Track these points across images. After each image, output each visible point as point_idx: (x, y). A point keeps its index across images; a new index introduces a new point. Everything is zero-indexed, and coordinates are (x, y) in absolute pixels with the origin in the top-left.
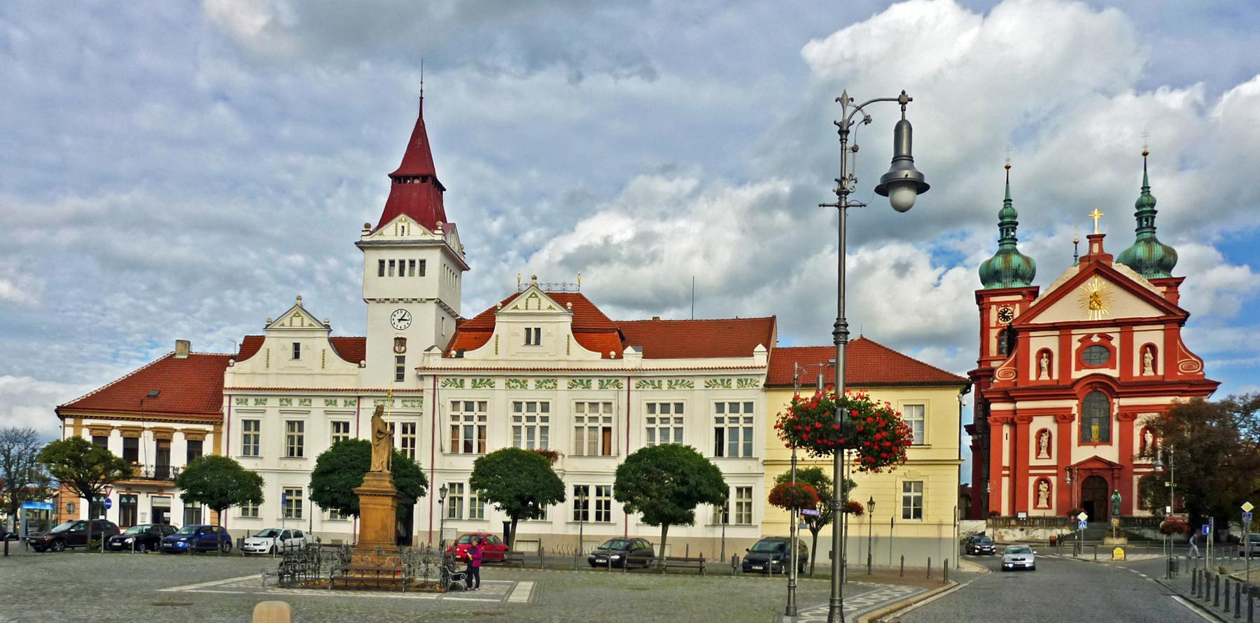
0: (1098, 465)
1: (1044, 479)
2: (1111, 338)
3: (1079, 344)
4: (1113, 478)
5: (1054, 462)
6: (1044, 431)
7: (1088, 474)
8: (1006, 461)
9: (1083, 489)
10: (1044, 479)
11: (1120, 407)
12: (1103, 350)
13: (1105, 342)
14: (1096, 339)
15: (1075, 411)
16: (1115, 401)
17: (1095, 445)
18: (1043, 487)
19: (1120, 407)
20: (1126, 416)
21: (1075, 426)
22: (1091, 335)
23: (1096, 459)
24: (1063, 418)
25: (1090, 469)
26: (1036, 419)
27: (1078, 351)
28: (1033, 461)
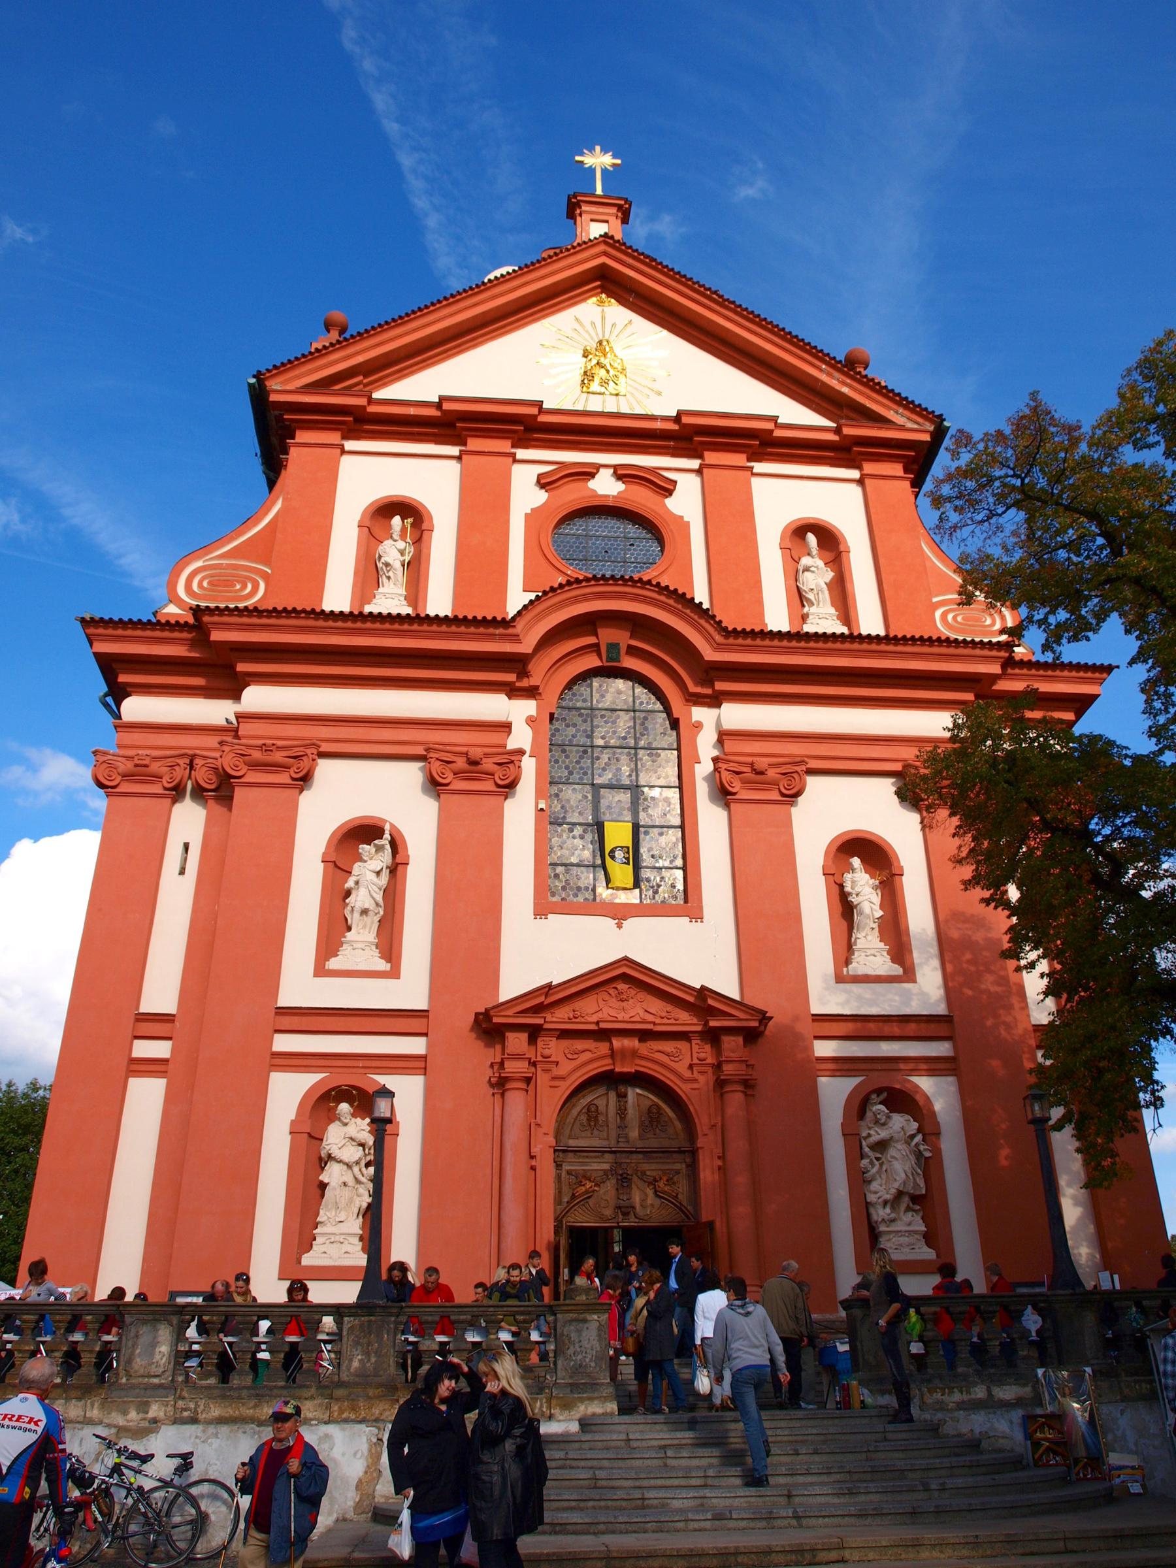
0: (640, 1010)
1: (350, 1091)
2: (667, 489)
3: (542, 496)
4: (720, 1084)
5: (411, 990)
6: (364, 832)
7: (590, 1058)
8: (161, 991)
9: (561, 1152)
10: (350, 1091)
11: (720, 741)
12: (632, 530)
13: (642, 499)
14: (605, 486)
15: (521, 738)
16: (699, 713)
17: (620, 914)
18: (346, 1135)
19: (724, 736)
20: (757, 776)
21: (519, 815)
22: (588, 473)
23: (627, 976)
24: (467, 772)
25: (603, 1035)
26: (330, 774)
27: (532, 518)
28: (299, 986)
